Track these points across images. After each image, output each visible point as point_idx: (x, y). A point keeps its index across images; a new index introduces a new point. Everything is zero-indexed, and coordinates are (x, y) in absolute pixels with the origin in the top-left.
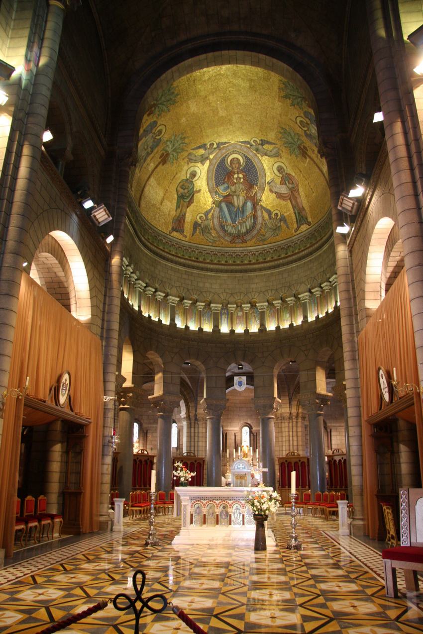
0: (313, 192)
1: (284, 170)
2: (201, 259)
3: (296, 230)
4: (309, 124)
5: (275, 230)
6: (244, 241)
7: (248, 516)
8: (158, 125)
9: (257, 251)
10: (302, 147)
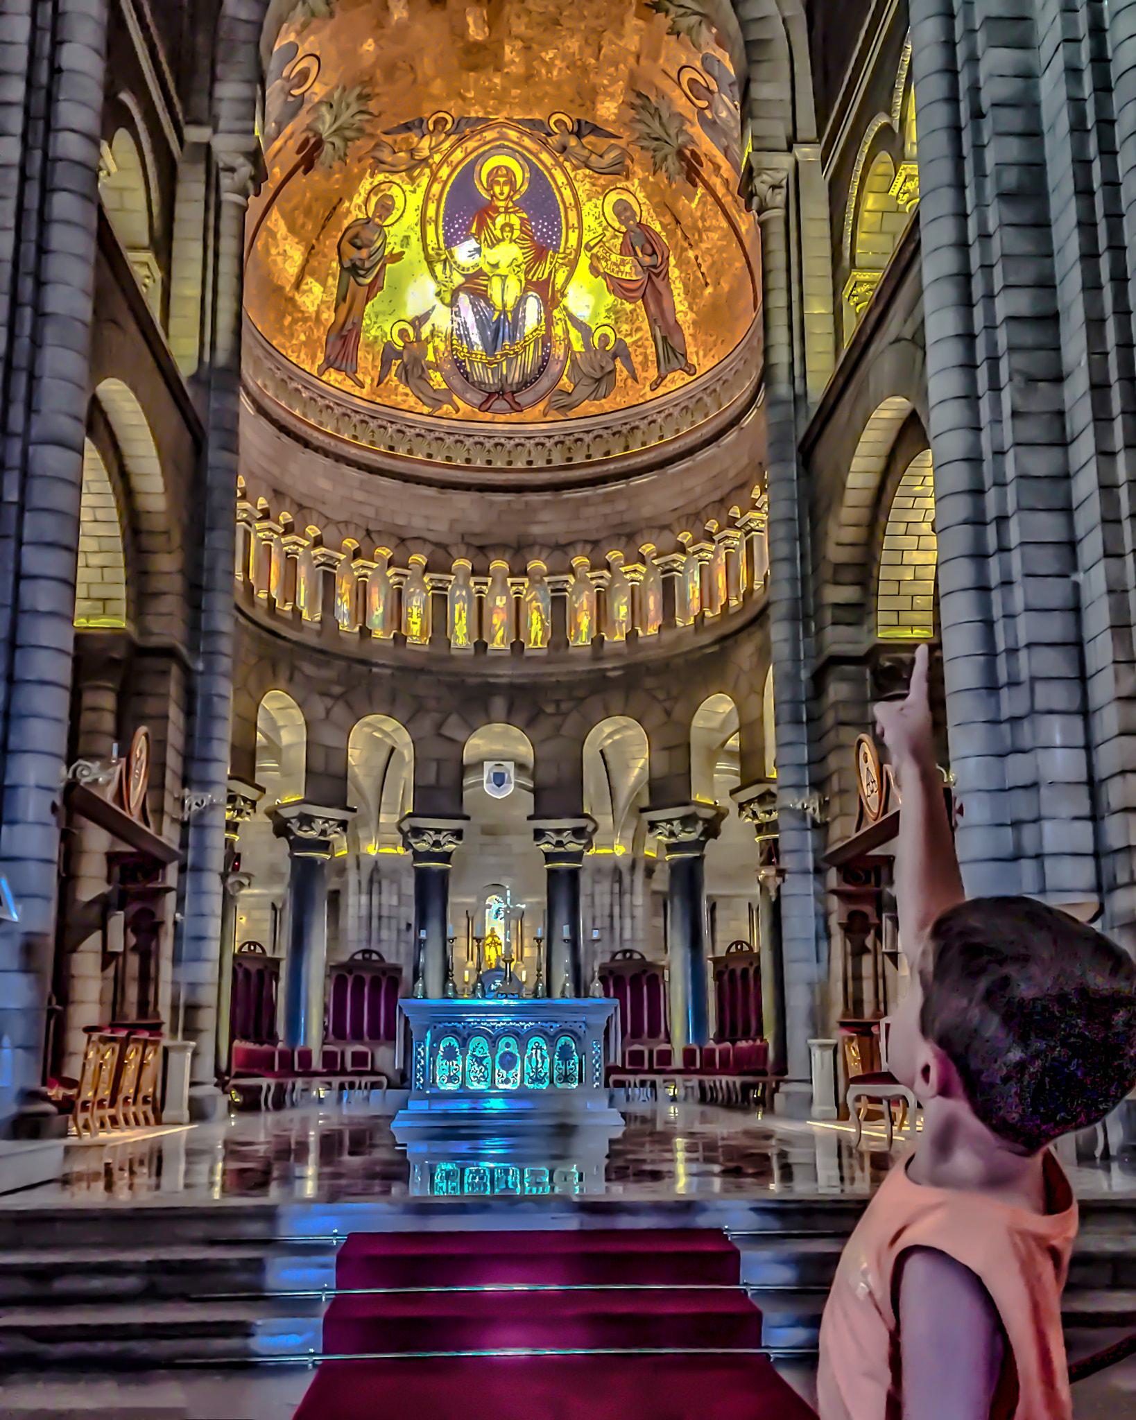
0: (707, 284)
1: (634, 213)
2: (401, 452)
3: (655, 386)
4: (712, 92)
5: (598, 380)
6: (517, 408)
8: (300, 54)
9: (549, 437)
10: (688, 153)
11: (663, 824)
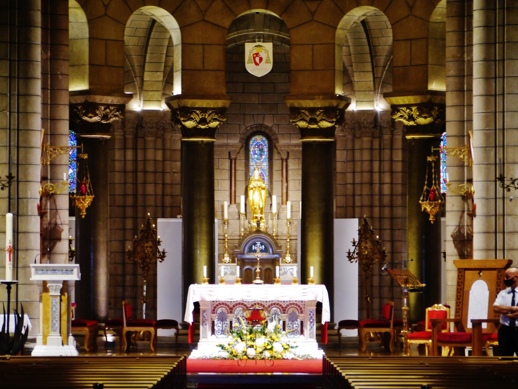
7: (290, 323)
11: (404, 109)
